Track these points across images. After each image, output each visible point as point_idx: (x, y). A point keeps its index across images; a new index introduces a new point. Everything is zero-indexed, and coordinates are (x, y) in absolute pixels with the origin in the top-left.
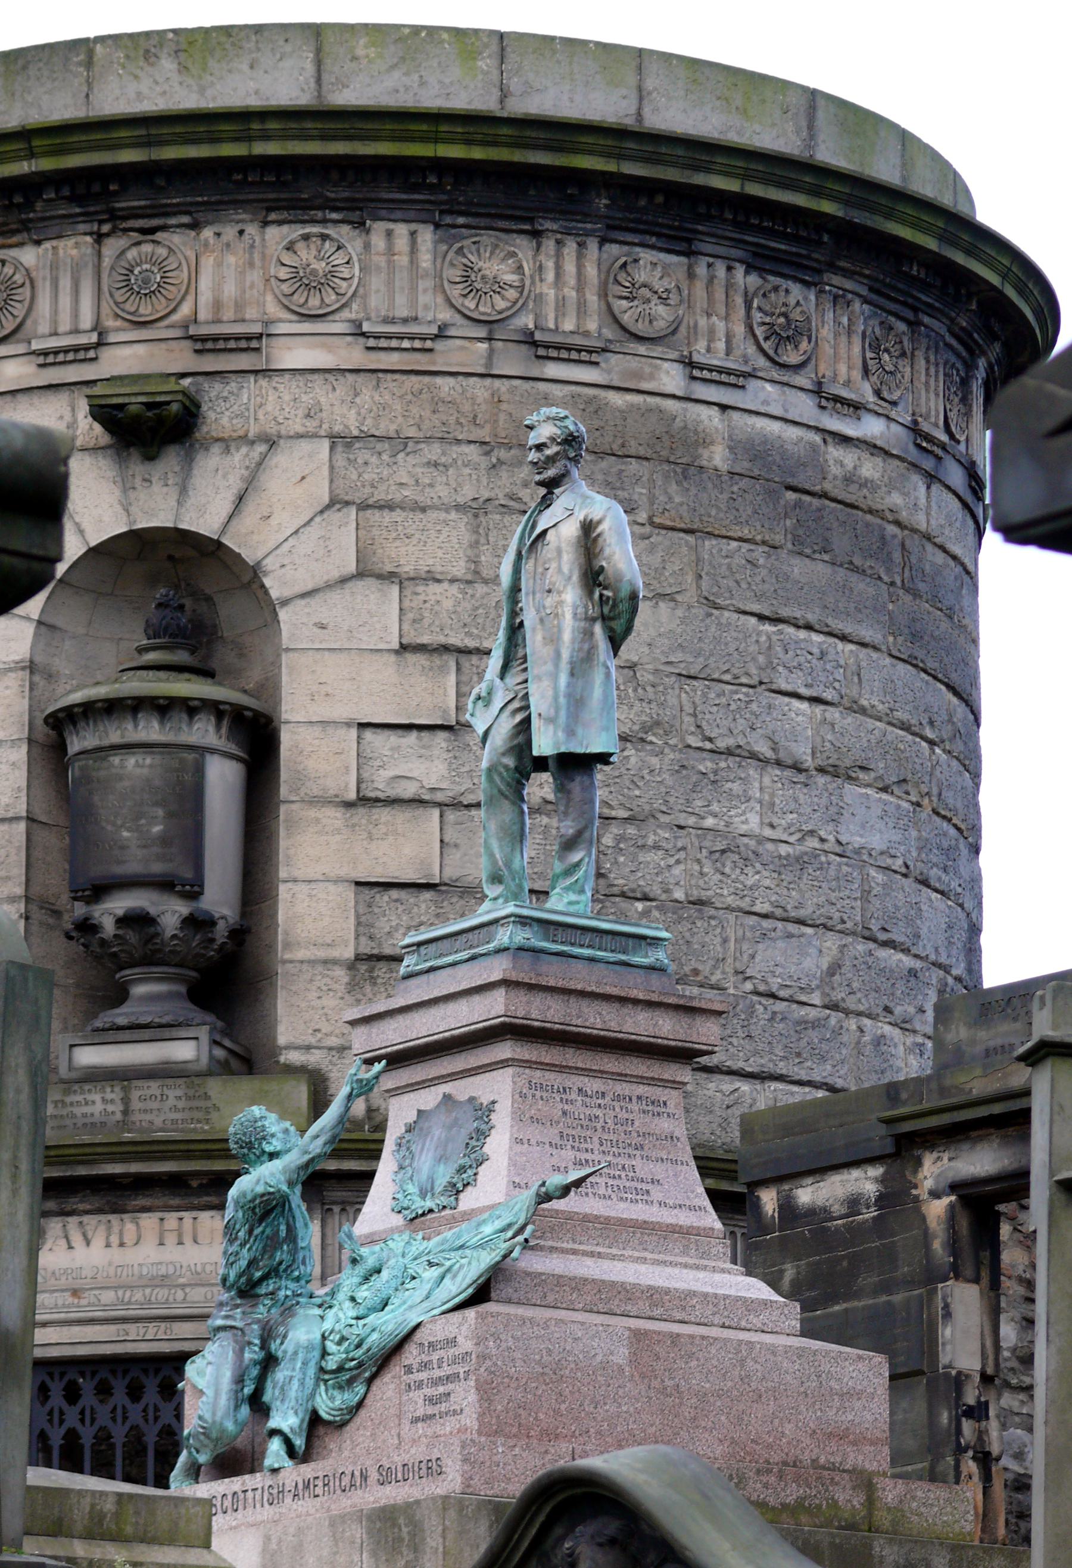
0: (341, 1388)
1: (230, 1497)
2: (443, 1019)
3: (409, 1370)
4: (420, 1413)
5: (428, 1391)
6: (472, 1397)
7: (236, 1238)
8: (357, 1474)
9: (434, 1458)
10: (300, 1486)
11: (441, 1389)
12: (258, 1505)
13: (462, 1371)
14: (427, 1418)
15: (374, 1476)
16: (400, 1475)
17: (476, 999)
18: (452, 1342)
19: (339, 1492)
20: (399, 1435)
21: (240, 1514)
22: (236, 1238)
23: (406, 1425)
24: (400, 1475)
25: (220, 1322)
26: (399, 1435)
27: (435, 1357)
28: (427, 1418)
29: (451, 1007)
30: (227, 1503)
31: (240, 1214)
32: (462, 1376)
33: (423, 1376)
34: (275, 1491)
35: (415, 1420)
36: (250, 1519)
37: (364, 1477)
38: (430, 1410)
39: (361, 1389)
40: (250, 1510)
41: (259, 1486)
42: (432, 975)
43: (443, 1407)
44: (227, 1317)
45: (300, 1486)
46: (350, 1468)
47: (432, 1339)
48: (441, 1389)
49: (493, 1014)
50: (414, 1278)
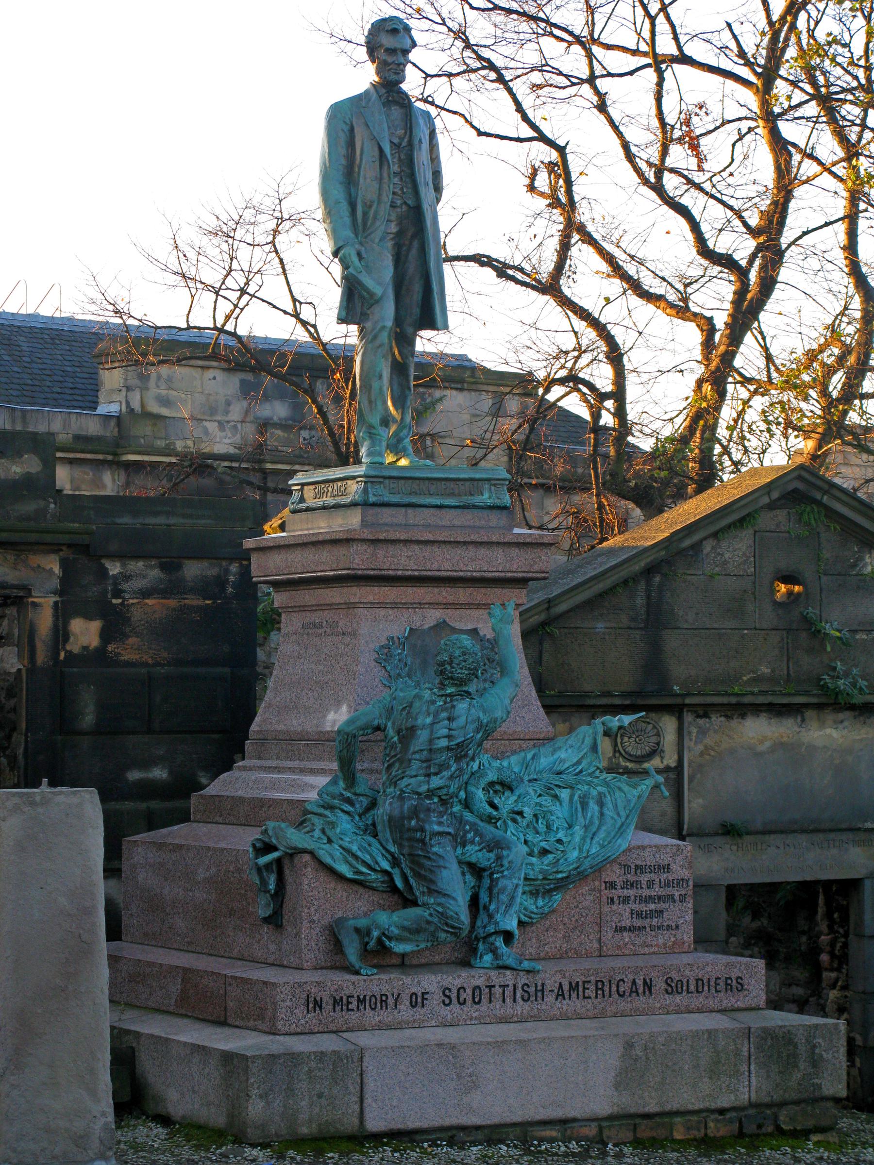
0: (534, 894)
1: (469, 991)
2: (473, 560)
3: (612, 885)
4: (627, 923)
5: (636, 907)
6: (689, 917)
7: (466, 755)
8: (640, 982)
9: (734, 976)
10: (566, 987)
11: (652, 907)
12: (508, 1000)
13: (677, 894)
14: (632, 929)
15: (660, 985)
16: (692, 988)
17: (515, 552)
18: (667, 868)
19: (615, 996)
20: (599, 940)
21: (484, 1006)
22: (466, 755)
23: (608, 935)
24: (692, 988)
25: (436, 828)
26: (599, 940)
27: (644, 878)
28: (632, 929)
29: (483, 551)
30: (467, 995)
31: (479, 735)
32: (677, 898)
33: (631, 892)
34: (532, 989)
35: (619, 930)
36: (499, 1013)
37: (648, 986)
38: (638, 923)
39: (558, 897)
40: (498, 1004)
41: (511, 983)
42: (410, 511)
43: (655, 921)
44: (440, 823)
45: (566, 987)
46: (631, 977)
47: (639, 863)
48: (652, 907)
49: (536, 568)
50: (540, 795)
